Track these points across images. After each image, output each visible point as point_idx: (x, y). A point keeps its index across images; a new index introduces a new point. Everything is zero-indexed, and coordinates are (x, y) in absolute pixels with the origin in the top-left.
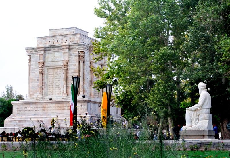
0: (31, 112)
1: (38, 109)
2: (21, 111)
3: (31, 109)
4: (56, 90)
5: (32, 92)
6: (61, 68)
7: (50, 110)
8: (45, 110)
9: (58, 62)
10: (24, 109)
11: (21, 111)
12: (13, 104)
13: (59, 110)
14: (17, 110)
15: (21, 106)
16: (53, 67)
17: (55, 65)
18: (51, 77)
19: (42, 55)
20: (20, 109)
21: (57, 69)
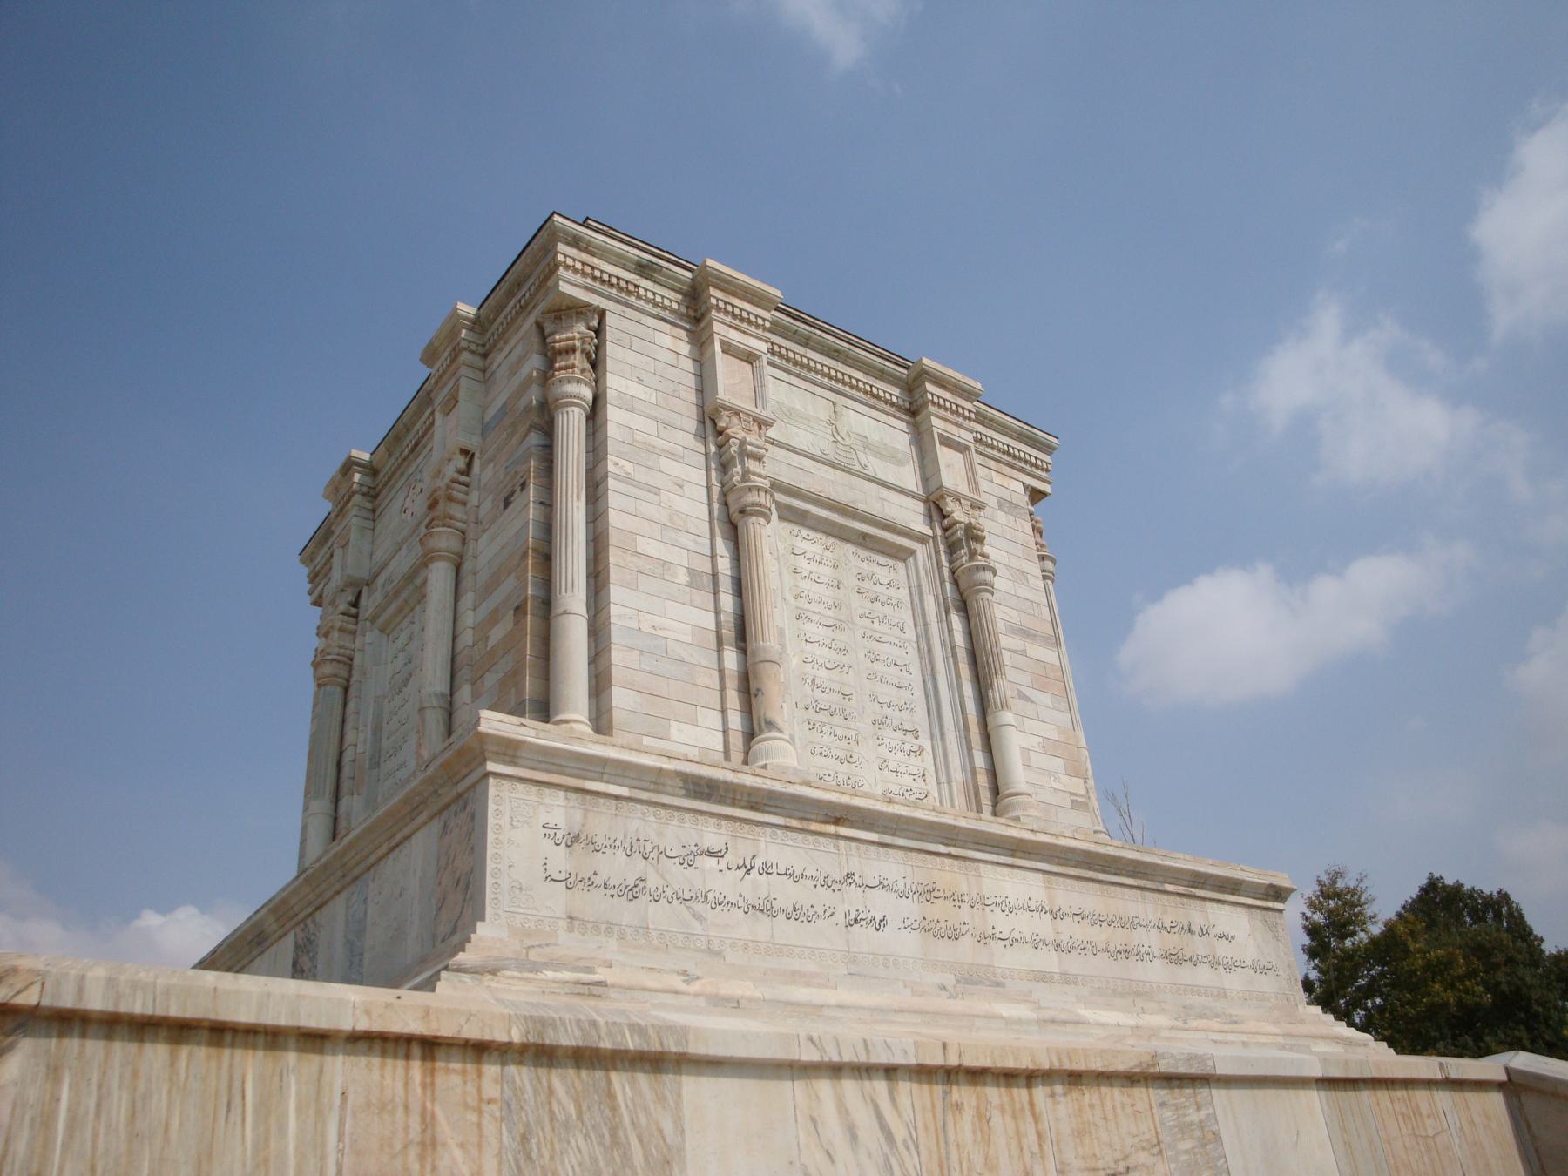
0: (785, 931)
1: (880, 904)
2: (632, 892)
3: (787, 894)
4: (883, 750)
5: (630, 687)
6: (901, 554)
7: (1011, 942)
8: (954, 935)
9: (885, 493)
10: (678, 877)
11: (632, 892)
12: (510, 750)
13: (1096, 951)
14: (560, 860)
15: (642, 823)
16: (835, 517)
17: (861, 506)
18: (814, 607)
19: (750, 358)
20: (615, 866)
21: (863, 553)
